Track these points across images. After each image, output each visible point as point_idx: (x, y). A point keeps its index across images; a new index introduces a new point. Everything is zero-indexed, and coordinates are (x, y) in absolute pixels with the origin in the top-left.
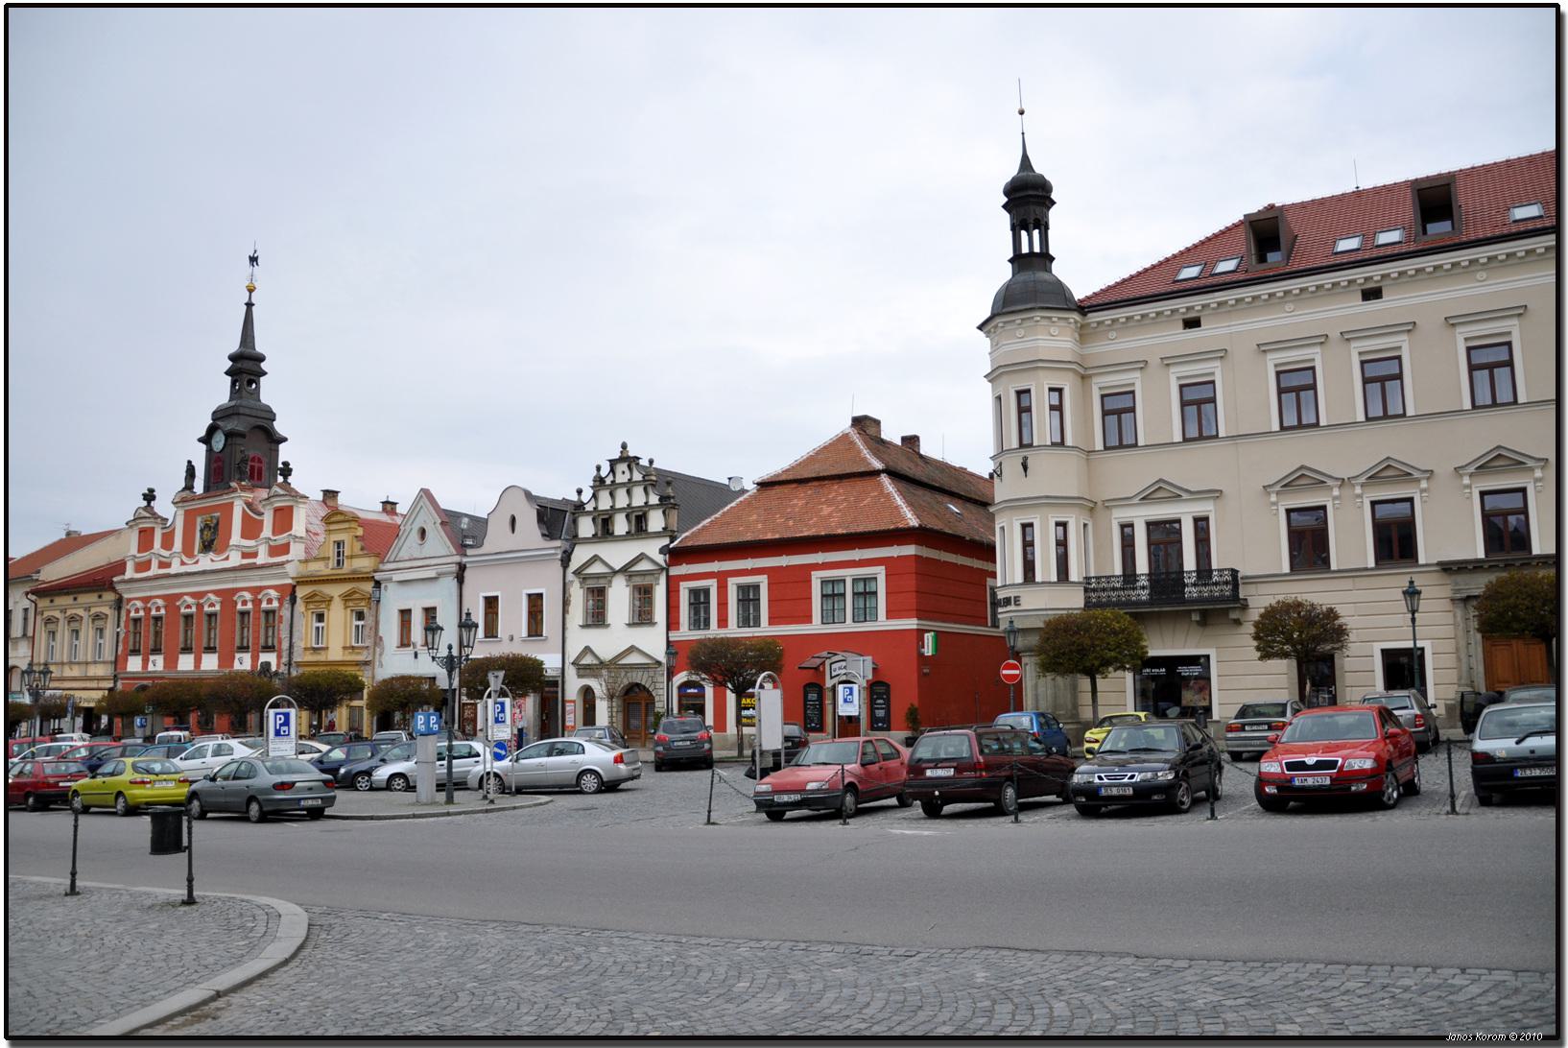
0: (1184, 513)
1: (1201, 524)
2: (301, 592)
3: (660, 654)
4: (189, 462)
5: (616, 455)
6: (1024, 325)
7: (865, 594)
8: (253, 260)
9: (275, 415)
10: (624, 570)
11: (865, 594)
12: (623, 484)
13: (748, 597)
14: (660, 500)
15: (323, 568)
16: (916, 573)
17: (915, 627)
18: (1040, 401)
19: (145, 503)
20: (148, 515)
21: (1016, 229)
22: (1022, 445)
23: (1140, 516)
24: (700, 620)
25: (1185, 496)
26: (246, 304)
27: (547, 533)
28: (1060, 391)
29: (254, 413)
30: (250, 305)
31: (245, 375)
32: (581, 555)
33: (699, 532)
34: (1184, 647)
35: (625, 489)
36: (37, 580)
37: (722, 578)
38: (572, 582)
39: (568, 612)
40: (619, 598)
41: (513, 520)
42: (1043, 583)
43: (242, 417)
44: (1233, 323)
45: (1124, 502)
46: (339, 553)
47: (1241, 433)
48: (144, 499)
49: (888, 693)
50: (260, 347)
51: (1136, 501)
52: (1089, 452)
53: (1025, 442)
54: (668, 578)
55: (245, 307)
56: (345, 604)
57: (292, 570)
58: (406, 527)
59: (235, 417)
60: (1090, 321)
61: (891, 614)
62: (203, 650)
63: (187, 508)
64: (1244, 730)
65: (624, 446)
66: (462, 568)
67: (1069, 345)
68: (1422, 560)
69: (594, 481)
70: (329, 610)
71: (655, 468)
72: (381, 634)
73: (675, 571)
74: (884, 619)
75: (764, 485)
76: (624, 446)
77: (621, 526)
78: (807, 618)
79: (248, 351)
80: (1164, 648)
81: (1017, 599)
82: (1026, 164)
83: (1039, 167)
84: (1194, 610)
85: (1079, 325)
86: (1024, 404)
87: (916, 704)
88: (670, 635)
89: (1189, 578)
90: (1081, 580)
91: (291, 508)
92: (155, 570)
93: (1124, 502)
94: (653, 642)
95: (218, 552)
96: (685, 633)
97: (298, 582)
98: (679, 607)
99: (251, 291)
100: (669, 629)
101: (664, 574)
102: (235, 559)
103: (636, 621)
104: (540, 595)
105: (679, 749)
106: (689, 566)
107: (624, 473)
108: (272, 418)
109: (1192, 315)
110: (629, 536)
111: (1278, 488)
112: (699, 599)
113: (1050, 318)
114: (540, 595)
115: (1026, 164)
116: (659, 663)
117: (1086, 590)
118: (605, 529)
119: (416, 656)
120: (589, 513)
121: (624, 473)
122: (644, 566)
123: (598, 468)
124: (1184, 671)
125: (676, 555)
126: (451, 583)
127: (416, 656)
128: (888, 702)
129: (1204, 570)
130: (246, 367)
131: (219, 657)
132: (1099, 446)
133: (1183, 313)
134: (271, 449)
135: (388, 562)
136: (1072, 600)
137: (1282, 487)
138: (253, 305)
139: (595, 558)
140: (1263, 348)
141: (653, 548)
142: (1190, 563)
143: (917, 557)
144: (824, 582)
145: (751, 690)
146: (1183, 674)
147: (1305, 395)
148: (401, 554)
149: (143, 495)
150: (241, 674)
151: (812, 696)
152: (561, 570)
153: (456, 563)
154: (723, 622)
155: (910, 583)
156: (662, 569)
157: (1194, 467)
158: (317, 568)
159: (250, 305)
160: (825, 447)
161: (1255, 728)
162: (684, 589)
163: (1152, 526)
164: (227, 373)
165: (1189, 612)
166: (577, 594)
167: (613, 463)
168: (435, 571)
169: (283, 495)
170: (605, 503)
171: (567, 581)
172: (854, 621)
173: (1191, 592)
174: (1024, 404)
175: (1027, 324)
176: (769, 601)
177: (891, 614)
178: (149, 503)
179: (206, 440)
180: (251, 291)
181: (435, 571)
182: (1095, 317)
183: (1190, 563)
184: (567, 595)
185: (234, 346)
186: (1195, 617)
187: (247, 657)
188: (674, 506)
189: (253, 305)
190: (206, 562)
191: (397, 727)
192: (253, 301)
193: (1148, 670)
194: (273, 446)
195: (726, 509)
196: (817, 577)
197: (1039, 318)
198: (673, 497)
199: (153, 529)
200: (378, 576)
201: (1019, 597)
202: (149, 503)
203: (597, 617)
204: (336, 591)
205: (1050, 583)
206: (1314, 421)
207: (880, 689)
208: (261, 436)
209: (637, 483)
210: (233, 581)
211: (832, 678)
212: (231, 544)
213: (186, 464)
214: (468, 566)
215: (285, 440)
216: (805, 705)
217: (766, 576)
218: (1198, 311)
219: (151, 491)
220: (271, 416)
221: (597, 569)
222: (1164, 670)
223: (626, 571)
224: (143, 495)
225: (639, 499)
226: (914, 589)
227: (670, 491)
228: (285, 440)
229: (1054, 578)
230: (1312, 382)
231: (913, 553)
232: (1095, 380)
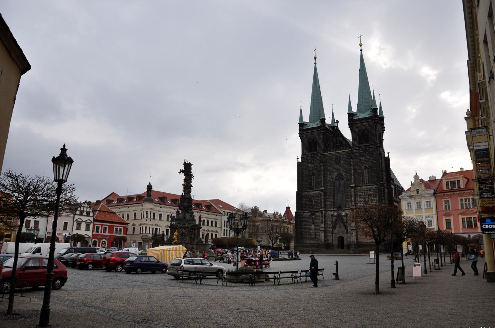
0: (158, 228)
1: (159, 229)
3: (91, 235)
5: (85, 202)
10: (85, 221)
11: (120, 230)
13: (105, 229)
22: (146, 218)
24: (97, 231)
32: (76, 217)
37: (102, 225)
40: (83, 226)
61: (123, 234)
73: (94, 223)
77: (85, 214)
78: (113, 233)
81: (148, 235)
94: (90, 233)
96: (95, 233)
100: (92, 232)
104: (67, 223)
110: (86, 216)
112: (98, 228)
114: (67, 223)
116: (90, 237)
118: (81, 213)
120: (78, 210)
122: (89, 221)
141: (92, 219)
142: (158, 233)
144: (115, 228)
152: (73, 219)
156: (92, 222)
157: (159, 223)
162: (96, 226)
166: (75, 224)
170: (82, 209)
173: (158, 236)
183: (158, 233)
196: (115, 227)
203: (78, 228)
221: (79, 220)
225: (88, 210)
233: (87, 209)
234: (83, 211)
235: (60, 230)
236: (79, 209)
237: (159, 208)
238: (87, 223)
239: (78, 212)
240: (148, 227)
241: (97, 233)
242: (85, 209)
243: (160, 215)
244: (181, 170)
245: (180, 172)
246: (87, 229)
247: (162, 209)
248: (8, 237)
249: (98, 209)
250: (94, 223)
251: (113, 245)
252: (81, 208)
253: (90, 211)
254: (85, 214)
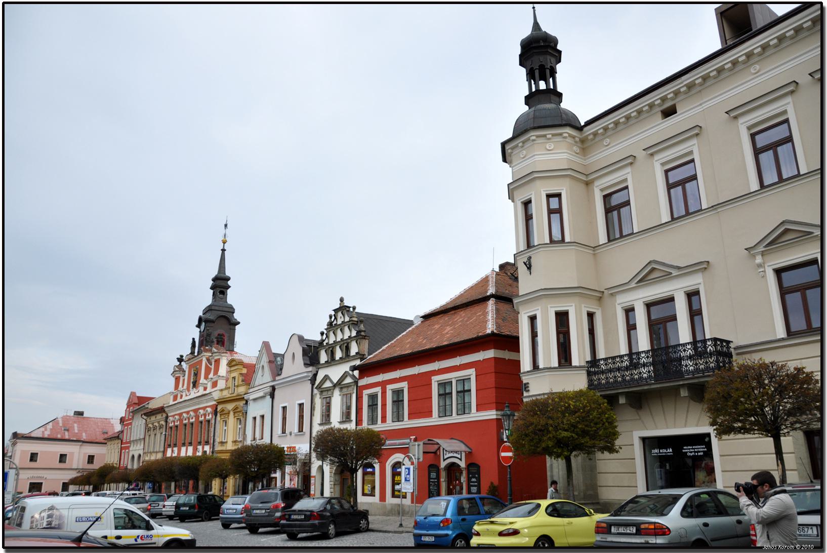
0: (677, 288)
1: (692, 295)
2: (219, 408)
4: (193, 339)
5: (338, 306)
6: (525, 147)
7: (464, 391)
8: (226, 226)
9: (234, 309)
16: (495, 372)
17: (495, 417)
18: (540, 210)
19: (178, 363)
20: (177, 369)
23: (639, 298)
25: (675, 273)
26: (222, 250)
27: (309, 363)
28: (559, 196)
29: (221, 309)
30: (223, 250)
31: (218, 288)
33: (384, 351)
34: (685, 426)
36: (148, 408)
37: (383, 384)
38: (316, 394)
39: (314, 415)
42: (544, 369)
43: (213, 311)
44: (705, 100)
45: (623, 288)
47: (721, 202)
48: (178, 361)
49: (479, 473)
50: (228, 273)
51: (633, 285)
52: (594, 248)
55: (221, 251)
56: (234, 415)
57: (216, 395)
59: (210, 312)
60: (585, 135)
61: (479, 408)
62: (182, 445)
63: (190, 364)
64: (609, 532)
65: (342, 300)
66: (273, 388)
67: (565, 156)
69: (328, 325)
70: (228, 419)
71: (356, 312)
72: (246, 433)
73: (362, 383)
75: (426, 317)
76: (342, 300)
77: (339, 354)
78: (429, 414)
79: (222, 275)
80: (657, 428)
82: (536, 25)
84: (683, 385)
85: (577, 139)
87: (496, 483)
89: (685, 350)
90: (583, 364)
91: (219, 359)
92: (179, 400)
93: (623, 288)
95: (197, 388)
97: (218, 402)
98: (362, 408)
99: (224, 242)
102: (201, 391)
103: (344, 420)
105: (257, 516)
106: (368, 378)
107: (341, 317)
108: (232, 311)
109: (668, 104)
111: (761, 248)
113: (545, 136)
115: (536, 25)
117: (589, 374)
121: (341, 317)
124: (689, 450)
126: (268, 398)
128: (479, 481)
130: (220, 285)
131: (193, 447)
132: (603, 238)
133: (659, 105)
134: (230, 329)
136: (576, 382)
137: (765, 247)
138: (225, 250)
139: (327, 378)
140: (733, 114)
143: (496, 360)
145: (398, 470)
146: (689, 454)
147: (782, 150)
148: (256, 383)
149: (178, 359)
150: (198, 457)
151: (433, 475)
153: (270, 386)
154: (384, 419)
155: (491, 380)
158: (226, 394)
159: (223, 250)
160: (472, 287)
161: (621, 530)
164: (211, 288)
165: (676, 389)
167: (336, 311)
171: (314, 394)
172: (457, 415)
175: (528, 145)
177: (479, 408)
178: (180, 363)
179: (199, 326)
180: (224, 242)
182: (590, 130)
184: (313, 404)
185: (215, 272)
186: (684, 393)
187: (190, 449)
188: (364, 337)
189: (225, 250)
190: (194, 393)
191: (273, 494)
192: (225, 248)
193: (656, 451)
194: (232, 327)
195: (399, 337)
196: (435, 379)
197: (534, 138)
198: (364, 331)
199: (179, 377)
200: (246, 397)
201: (528, 383)
202: (180, 363)
204: (230, 407)
205: (550, 368)
206: (796, 173)
207: (473, 469)
208: (224, 321)
210: (199, 404)
211: (444, 460)
212: (200, 382)
213: (192, 340)
215: (239, 323)
216: (429, 482)
218: (672, 99)
219: (182, 356)
220: (232, 310)
221: (328, 384)
222: (671, 450)
224: (178, 359)
226: (494, 386)
227: (362, 327)
228: (239, 323)
229: (555, 363)
230: (789, 134)
231: (493, 356)
232: (597, 183)
240: (578, 313)
251: (438, 477)
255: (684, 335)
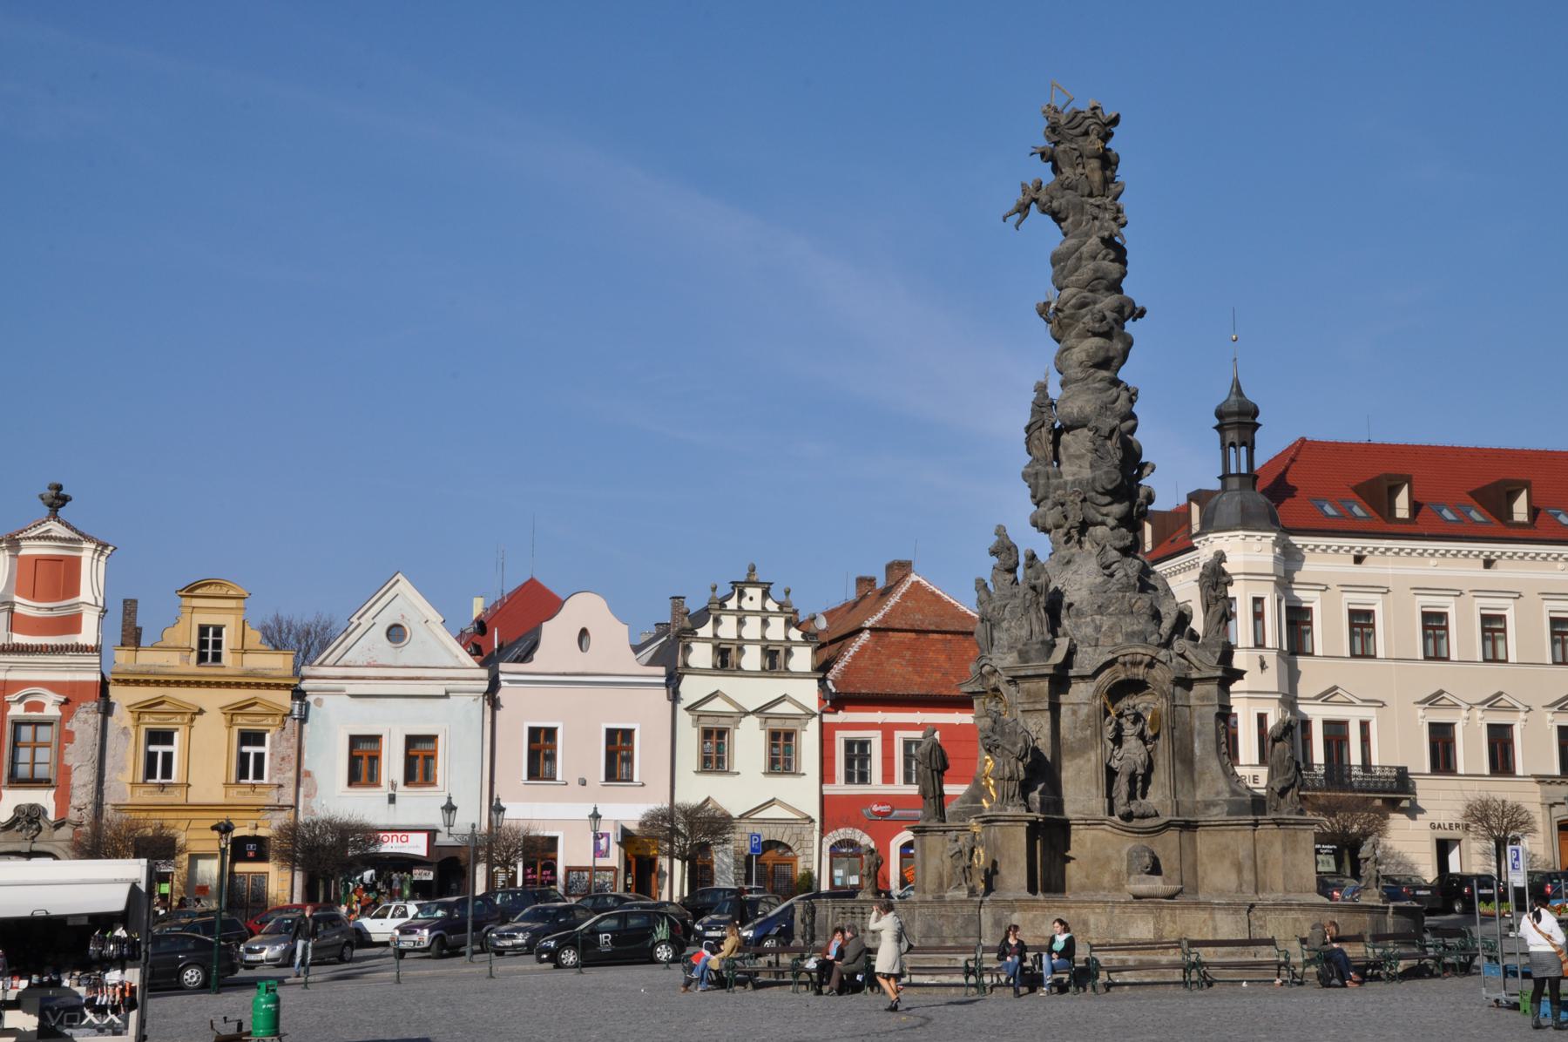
0: (1353, 716)
1: (1364, 726)
2: (117, 694)
10: (758, 711)
12: (754, 613)
14: (803, 636)
15: (177, 662)
21: (1225, 447)
32: (692, 689)
35: (758, 620)
37: (888, 730)
40: (749, 743)
41: (584, 633)
46: (203, 644)
51: (1319, 701)
53: (1259, 643)
54: (822, 725)
58: (362, 620)
68: (1519, 771)
73: (828, 718)
74: (843, 782)
76: (753, 569)
77: (752, 658)
82: (1237, 389)
83: (1251, 395)
86: (1259, 609)
88: (824, 787)
96: (839, 787)
98: (834, 758)
100: (822, 781)
101: (816, 720)
112: (858, 754)
115: (1237, 389)
118: (726, 659)
119: (392, 799)
120: (705, 640)
123: (714, 589)
125: (837, 701)
127: (392, 799)
129: (1366, 765)
135: (321, 664)
139: (714, 695)
141: (807, 693)
156: (814, 715)
157: (1355, 677)
162: (840, 737)
163: (1326, 723)
168: (443, 687)
169: (61, 539)
170: (728, 629)
174: (1259, 609)
176: (883, 758)
181: (443, 687)
203: (714, 759)
204: (214, 700)
209: (773, 614)
214: (503, 684)
217: (880, 732)
223: (761, 712)
225: (777, 630)
233: (765, 623)
234: (741, 644)
235: (583, 783)
236: (706, 631)
237: (1475, 570)
238: (776, 725)
239: (701, 655)
241: (857, 789)
242: (752, 629)
243: (1492, 626)
244: (1024, 187)
245: (1023, 209)
246: (781, 756)
247: (1374, 569)
248: (251, 854)
249: (868, 624)
250: (828, 718)
252: (717, 622)
253: (787, 638)
254: (752, 658)
255: (1355, 758)
